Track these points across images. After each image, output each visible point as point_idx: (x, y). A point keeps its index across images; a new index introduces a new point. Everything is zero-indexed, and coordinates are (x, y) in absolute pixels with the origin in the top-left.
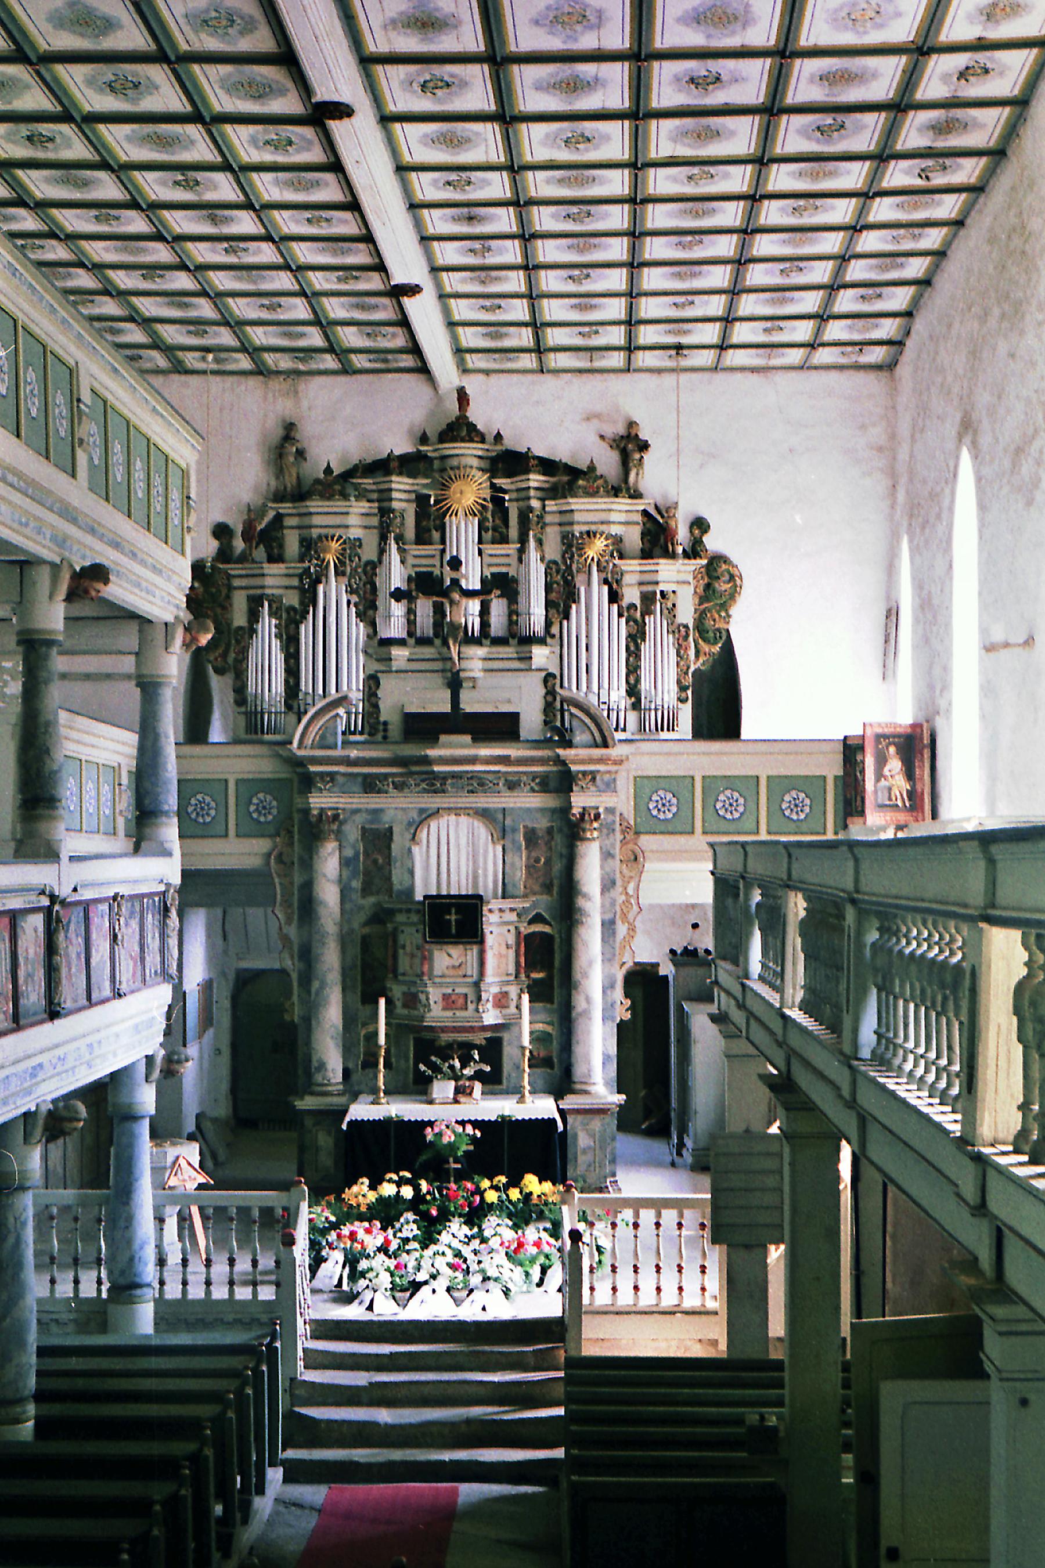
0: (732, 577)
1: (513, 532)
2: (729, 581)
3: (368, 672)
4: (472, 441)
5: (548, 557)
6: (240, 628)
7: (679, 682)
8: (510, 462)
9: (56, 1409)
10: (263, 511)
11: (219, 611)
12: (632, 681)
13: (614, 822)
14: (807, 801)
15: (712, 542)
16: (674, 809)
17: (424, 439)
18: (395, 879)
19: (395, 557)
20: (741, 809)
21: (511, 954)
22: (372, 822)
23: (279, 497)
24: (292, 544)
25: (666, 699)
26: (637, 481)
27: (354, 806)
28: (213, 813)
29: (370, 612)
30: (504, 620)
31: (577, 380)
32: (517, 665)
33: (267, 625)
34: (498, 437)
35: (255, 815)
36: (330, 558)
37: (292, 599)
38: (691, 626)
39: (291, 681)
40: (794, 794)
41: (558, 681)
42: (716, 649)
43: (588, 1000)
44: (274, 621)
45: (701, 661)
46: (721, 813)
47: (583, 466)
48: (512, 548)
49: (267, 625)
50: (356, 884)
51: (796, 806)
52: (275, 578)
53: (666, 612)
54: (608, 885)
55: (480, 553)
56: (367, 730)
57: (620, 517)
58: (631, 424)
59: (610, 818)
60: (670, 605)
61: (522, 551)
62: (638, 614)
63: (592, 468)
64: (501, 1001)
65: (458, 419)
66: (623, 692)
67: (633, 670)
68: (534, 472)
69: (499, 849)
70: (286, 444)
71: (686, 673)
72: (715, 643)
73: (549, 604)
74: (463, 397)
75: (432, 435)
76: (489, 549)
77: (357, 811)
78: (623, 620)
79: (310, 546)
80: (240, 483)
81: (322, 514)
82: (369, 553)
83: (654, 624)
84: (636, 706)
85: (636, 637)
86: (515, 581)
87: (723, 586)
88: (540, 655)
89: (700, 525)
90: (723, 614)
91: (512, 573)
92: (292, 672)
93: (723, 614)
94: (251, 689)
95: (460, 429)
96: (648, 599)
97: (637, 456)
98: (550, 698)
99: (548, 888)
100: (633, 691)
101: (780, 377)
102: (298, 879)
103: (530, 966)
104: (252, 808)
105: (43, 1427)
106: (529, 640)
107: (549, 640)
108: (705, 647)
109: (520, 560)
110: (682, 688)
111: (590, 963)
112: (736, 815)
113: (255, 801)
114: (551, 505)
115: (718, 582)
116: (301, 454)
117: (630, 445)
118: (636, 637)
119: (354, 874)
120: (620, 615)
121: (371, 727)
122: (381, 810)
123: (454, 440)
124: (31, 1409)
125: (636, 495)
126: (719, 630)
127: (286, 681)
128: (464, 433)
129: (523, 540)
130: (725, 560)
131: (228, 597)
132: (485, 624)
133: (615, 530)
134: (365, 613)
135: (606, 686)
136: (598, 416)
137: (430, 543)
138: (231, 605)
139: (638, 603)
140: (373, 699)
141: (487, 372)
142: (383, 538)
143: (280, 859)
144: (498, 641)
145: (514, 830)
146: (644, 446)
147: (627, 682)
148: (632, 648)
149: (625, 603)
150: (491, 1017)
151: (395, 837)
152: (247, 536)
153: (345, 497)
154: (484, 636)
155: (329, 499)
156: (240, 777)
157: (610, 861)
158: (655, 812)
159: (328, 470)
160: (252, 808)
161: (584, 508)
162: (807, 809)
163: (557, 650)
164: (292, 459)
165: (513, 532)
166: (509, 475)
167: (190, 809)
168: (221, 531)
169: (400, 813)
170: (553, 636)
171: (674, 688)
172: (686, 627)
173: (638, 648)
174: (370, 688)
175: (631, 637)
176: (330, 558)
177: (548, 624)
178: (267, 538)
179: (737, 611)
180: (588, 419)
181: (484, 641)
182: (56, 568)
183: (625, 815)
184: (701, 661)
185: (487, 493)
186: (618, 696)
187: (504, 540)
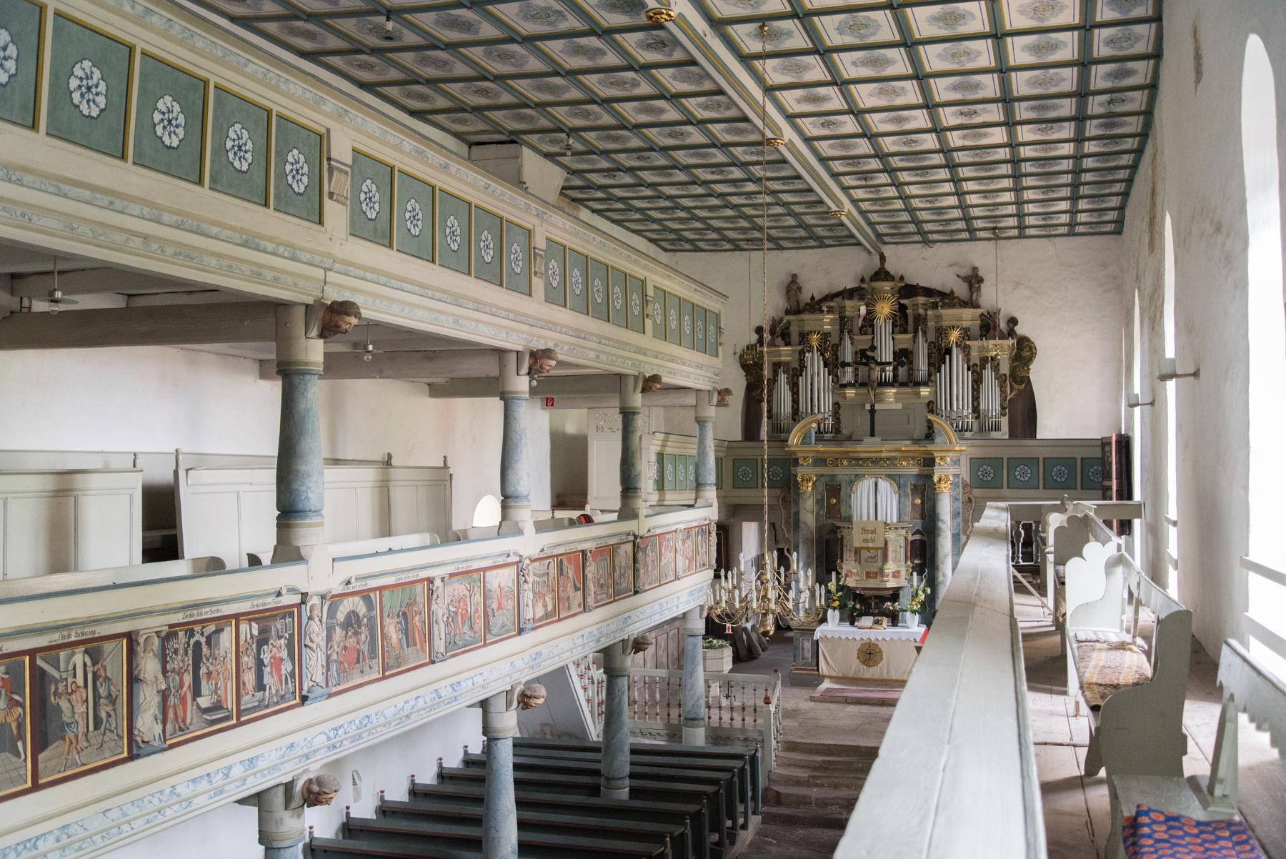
0: (1031, 349)
1: (911, 327)
8: (910, 290)
9: (639, 783)
10: (781, 320)
15: (1020, 330)
17: (863, 280)
19: (847, 341)
21: (903, 551)
23: (788, 312)
24: (795, 338)
30: (906, 373)
31: (944, 245)
33: (782, 378)
34: (902, 278)
36: (815, 344)
37: (796, 365)
43: (944, 575)
47: (948, 291)
48: (910, 336)
49: (782, 378)
50: (823, 513)
52: (786, 353)
54: (955, 515)
57: (968, 317)
58: (975, 269)
61: (915, 337)
63: (952, 292)
64: (896, 575)
67: (976, 398)
70: (792, 286)
73: (930, 365)
74: (883, 258)
75: (867, 278)
76: (898, 336)
77: (820, 476)
79: (804, 337)
80: (769, 306)
82: (834, 339)
83: (988, 374)
84: (977, 418)
85: (977, 382)
86: (912, 352)
87: (1026, 354)
88: (925, 391)
89: (1013, 321)
92: (795, 401)
94: (774, 410)
95: (882, 274)
96: (984, 361)
99: (923, 517)
100: (976, 410)
101: (1057, 240)
102: (793, 510)
103: (913, 557)
105: (634, 792)
106: (918, 384)
108: (1016, 386)
110: (1003, 408)
111: (946, 556)
114: (929, 312)
115: (1024, 352)
116: (800, 289)
117: (974, 280)
118: (977, 382)
119: (821, 508)
123: (877, 280)
124: (627, 782)
125: (977, 306)
129: (916, 332)
132: (895, 376)
133: (965, 324)
136: (956, 264)
137: (866, 334)
142: (842, 331)
143: (784, 499)
144: (903, 385)
145: (905, 486)
146: (981, 280)
150: (891, 583)
152: (772, 332)
153: (822, 311)
154: (895, 382)
159: (813, 298)
161: (949, 315)
165: (911, 327)
166: (907, 298)
168: (759, 330)
171: (998, 408)
175: (975, 381)
176: (815, 344)
177: (930, 375)
178: (780, 332)
179: (1033, 367)
180: (951, 266)
182: (636, 377)
186: (968, 411)
187: (905, 331)
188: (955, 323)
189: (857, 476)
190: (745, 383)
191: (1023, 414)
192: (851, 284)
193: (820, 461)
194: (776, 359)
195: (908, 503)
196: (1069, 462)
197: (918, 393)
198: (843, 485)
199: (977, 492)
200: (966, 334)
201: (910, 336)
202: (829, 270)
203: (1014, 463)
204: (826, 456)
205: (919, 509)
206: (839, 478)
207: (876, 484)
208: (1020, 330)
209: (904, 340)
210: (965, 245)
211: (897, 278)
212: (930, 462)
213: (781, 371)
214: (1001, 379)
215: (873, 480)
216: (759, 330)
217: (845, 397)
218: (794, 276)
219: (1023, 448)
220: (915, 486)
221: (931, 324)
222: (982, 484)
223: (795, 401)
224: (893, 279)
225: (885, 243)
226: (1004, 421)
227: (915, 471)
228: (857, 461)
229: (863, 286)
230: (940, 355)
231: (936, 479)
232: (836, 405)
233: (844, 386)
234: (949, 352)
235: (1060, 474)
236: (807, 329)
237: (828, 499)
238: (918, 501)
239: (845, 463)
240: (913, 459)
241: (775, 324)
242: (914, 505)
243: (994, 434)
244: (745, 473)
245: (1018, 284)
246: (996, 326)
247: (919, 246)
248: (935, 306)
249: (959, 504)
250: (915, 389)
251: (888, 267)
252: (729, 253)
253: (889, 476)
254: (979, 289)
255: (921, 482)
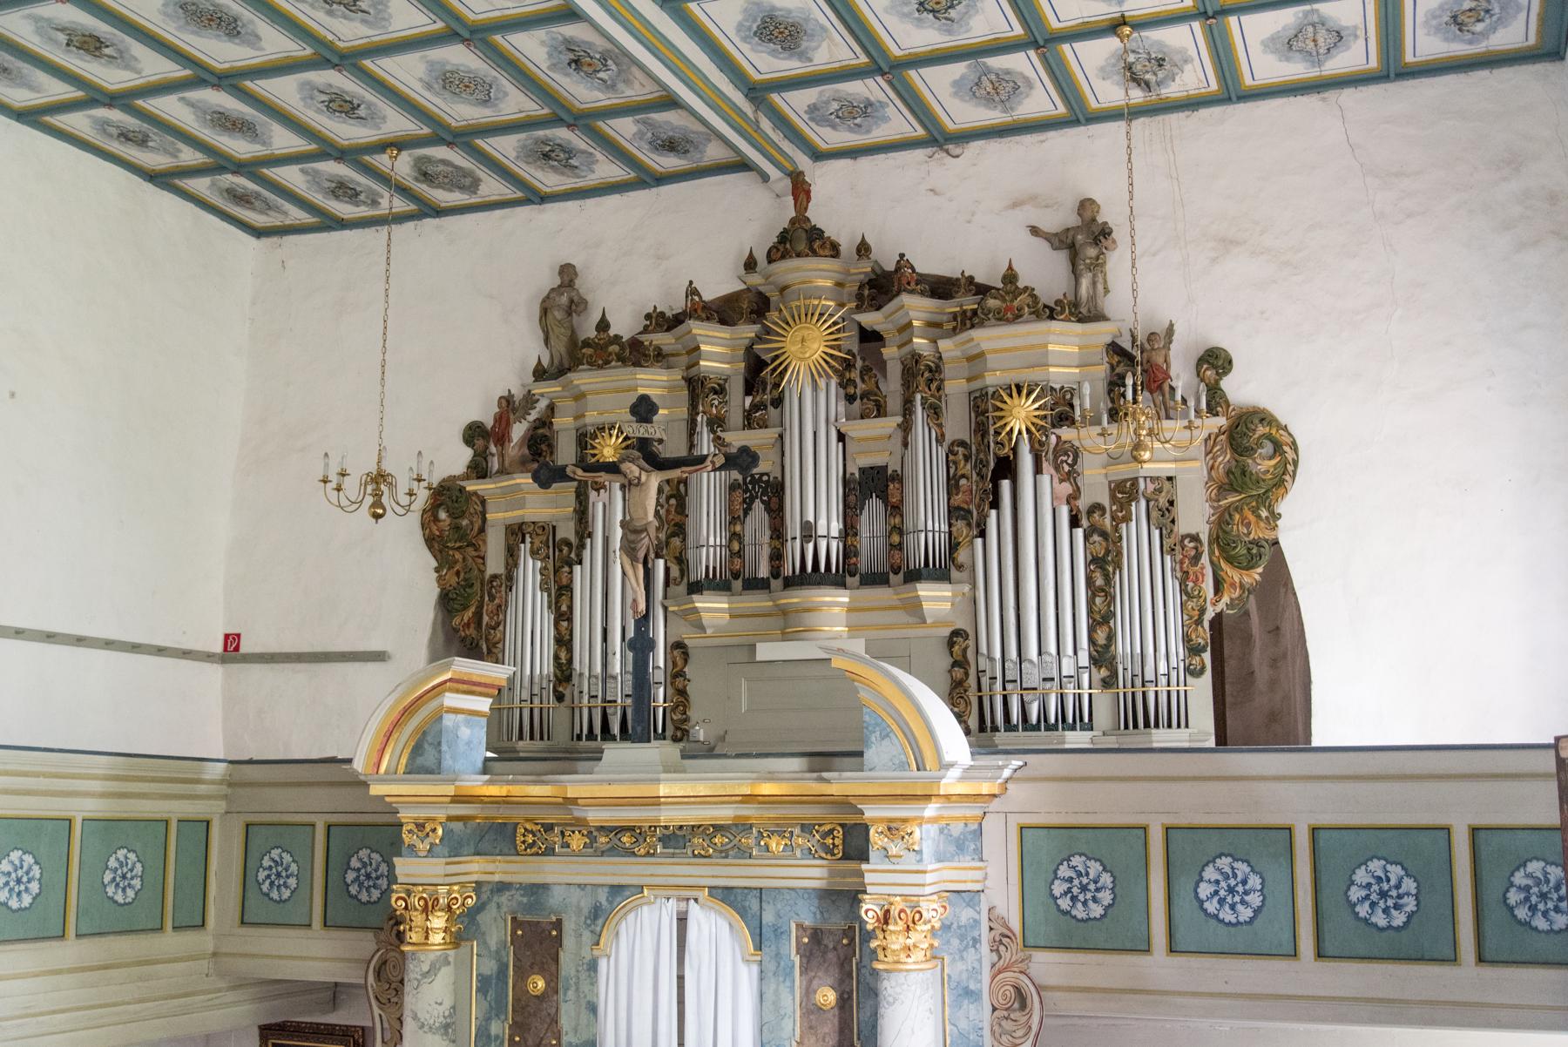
0: (1278, 447)
2: (1271, 458)
3: (671, 640)
4: (815, 254)
5: (949, 438)
6: (495, 577)
7: (1187, 639)
10: (530, 400)
11: (471, 551)
12: (1101, 636)
13: (977, 922)
14: (1409, 885)
15: (1240, 389)
16: (1106, 897)
17: (750, 264)
18: (565, 1022)
20: (1255, 899)
22: (529, 908)
23: (540, 374)
25: (1162, 669)
26: (1093, 298)
27: (497, 878)
28: (292, 882)
29: (676, 541)
30: (880, 543)
31: (994, 146)
32: (901, 617)
33: (530, 570)
34: (863, 249)
35: (353, 890)
37: (567, 531)
38: (1204, 538)
39: (563, 655)
40: (1376, 866)
41: (971, 642)
42: (1256, 574)
44: (539, 564)
45: (1226, 599)
46: (1211, 907)
48: (890, 423)
49: (530, 570)
51: (1383, 895)
53: (1155, 514)
55: (841, 437)
56: (669, 733)
57: (1066, 354)
58: (1086, 206)
59: (966, 915)
60: (1163, 501)
61: (906, 427)
62: (1107, 522)
63: (1010, 277)
65: (793, 221)
66: (1084, 660)
67: (1101, 619)
68: (912, 292)
69: (755, 968)
70: (563, 300)
71: (1199, 622)
72: (1248, 568)
73: (954, 512)
74: (801, 190)
75: (761, 257)
77: (502, 887)
78: (1079, 533)
81: (605, 394)
83: (1138, 536)
84: (1108, 683)
86: (898, 478)
87: (1262, 464)
88: (936, 598)
89: (1215, 361)
90: (1264, 513)
91: (894, 466)
92: (564, 642)
93: (1264, 513)
95: (800, 238)
96: (1124, 492)
97: (1092, 252)
98: (958, 673)
100: (1102, 656)
101: (1348, 95)
104: (351, 876)
107: (954, 574)
108: (1231, 573)
109: (905, 445)
110: (1193, 650)
112: (1245, 914)
113: (355, 863)
114: (945, 345)
115: (1253, 457)
116: (576, 306)
117: (1084, 240)
119: (497, 1009)
120: (1074, 522)
121: (677, 728)
122: (545, 887)
123: (783, 257)
126: (1256, 543)
127: (556, 657)
128: (802, 246)
130: (1265, 417)
131: (482, 530)
132: (849, 552)
133: (1059, 375)
134: (667, 544)
135: (1053, 649)
136: (1033, 199)
138: (485, 542)
139: (1106, 502)
140: (679, 682)
141: (853, 153)
145: (779, 933)
146: (1101, 235)
147: (1092, 641)
148: (1099, 582)
149: (1083, 504)
151: (569, 941)
155: (600, 367)
156: (334, 819)
157: (970, 1008)
158: (1065, 903)
159: (603, 325)
160: (351, 876)
162: (1410, 904)
163: (966, 588)
164: (559, 315)
167: (262, 875)
168: (474, 434)
169: (577, 892)
170: (960, 567)
171: (1177, 649)
172: (1195, 538)
173: (1108, 579)
174: (675, 664)
175: (1096, 562)
177: (953, 546)
180: (1016, 205)
181: (849, 580)
183: (1001, 910)
184: (1226, 599)
185: (851, 341)
188: (1026, 376)
189: (617, 890)
190: (434, 591)
191: (1254, 669)
192: (718, 283)
193: (495, 833)
194: (514, 516)
195: (791, 1002)
196: (1419, 846)
197: (915, 607)
198: (569, 926)
199: (1047, 966)
200: (1062, 411)
201: (890, 423)
202: (661, 248)
203: (1190, 846)
204: (516, 814)
205: (829, 1028)
206: (556, 898)
207: (682, 920)
208: (1240, 389)
209: (875, 439)
210: (1057, 140)
211: (847, 244)
212: (853, 844)
213: (524, 548)
214: (1183, 551)
215: (671, 908)
216: (474, 434)
217: (701, 627)
218: (568, 273)
219: (1264, 786)
220: (816, 935)
221: (955, 387)
222: (1073, 936)
223: (564, 642)
224: (835, 251)
225: (818, 155)
226: (1201, 692)
227: (813, 874)
228: (620, 839)
229: (755, 280)
230: (986, 473)
231: (869, 911)
232: (678, 648)
233: (695, 588)
234: (1007, 468)
235: (1383, 893)
236: (592, 418)
237: (522, 974)
238: (827, 996)
239: (577, 842)
240: (807, 828)
241: (509, 408)
242: (811, 1011)
243: (1161, 737)
244: (278, 875)
245: (1227, 244)
246: (1155, 380)
247: (919, 154)
248: (967, 321)
249: (982, 1014)
250: (905, 592)
251: (817, 214)
252: (410, 225)
253: (726, 896)
254: (1097, 265)
255: (837, 922)
